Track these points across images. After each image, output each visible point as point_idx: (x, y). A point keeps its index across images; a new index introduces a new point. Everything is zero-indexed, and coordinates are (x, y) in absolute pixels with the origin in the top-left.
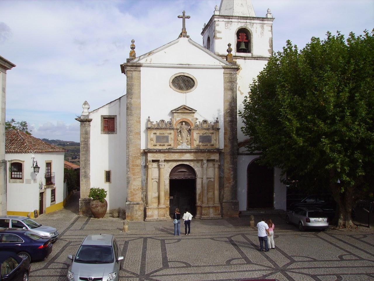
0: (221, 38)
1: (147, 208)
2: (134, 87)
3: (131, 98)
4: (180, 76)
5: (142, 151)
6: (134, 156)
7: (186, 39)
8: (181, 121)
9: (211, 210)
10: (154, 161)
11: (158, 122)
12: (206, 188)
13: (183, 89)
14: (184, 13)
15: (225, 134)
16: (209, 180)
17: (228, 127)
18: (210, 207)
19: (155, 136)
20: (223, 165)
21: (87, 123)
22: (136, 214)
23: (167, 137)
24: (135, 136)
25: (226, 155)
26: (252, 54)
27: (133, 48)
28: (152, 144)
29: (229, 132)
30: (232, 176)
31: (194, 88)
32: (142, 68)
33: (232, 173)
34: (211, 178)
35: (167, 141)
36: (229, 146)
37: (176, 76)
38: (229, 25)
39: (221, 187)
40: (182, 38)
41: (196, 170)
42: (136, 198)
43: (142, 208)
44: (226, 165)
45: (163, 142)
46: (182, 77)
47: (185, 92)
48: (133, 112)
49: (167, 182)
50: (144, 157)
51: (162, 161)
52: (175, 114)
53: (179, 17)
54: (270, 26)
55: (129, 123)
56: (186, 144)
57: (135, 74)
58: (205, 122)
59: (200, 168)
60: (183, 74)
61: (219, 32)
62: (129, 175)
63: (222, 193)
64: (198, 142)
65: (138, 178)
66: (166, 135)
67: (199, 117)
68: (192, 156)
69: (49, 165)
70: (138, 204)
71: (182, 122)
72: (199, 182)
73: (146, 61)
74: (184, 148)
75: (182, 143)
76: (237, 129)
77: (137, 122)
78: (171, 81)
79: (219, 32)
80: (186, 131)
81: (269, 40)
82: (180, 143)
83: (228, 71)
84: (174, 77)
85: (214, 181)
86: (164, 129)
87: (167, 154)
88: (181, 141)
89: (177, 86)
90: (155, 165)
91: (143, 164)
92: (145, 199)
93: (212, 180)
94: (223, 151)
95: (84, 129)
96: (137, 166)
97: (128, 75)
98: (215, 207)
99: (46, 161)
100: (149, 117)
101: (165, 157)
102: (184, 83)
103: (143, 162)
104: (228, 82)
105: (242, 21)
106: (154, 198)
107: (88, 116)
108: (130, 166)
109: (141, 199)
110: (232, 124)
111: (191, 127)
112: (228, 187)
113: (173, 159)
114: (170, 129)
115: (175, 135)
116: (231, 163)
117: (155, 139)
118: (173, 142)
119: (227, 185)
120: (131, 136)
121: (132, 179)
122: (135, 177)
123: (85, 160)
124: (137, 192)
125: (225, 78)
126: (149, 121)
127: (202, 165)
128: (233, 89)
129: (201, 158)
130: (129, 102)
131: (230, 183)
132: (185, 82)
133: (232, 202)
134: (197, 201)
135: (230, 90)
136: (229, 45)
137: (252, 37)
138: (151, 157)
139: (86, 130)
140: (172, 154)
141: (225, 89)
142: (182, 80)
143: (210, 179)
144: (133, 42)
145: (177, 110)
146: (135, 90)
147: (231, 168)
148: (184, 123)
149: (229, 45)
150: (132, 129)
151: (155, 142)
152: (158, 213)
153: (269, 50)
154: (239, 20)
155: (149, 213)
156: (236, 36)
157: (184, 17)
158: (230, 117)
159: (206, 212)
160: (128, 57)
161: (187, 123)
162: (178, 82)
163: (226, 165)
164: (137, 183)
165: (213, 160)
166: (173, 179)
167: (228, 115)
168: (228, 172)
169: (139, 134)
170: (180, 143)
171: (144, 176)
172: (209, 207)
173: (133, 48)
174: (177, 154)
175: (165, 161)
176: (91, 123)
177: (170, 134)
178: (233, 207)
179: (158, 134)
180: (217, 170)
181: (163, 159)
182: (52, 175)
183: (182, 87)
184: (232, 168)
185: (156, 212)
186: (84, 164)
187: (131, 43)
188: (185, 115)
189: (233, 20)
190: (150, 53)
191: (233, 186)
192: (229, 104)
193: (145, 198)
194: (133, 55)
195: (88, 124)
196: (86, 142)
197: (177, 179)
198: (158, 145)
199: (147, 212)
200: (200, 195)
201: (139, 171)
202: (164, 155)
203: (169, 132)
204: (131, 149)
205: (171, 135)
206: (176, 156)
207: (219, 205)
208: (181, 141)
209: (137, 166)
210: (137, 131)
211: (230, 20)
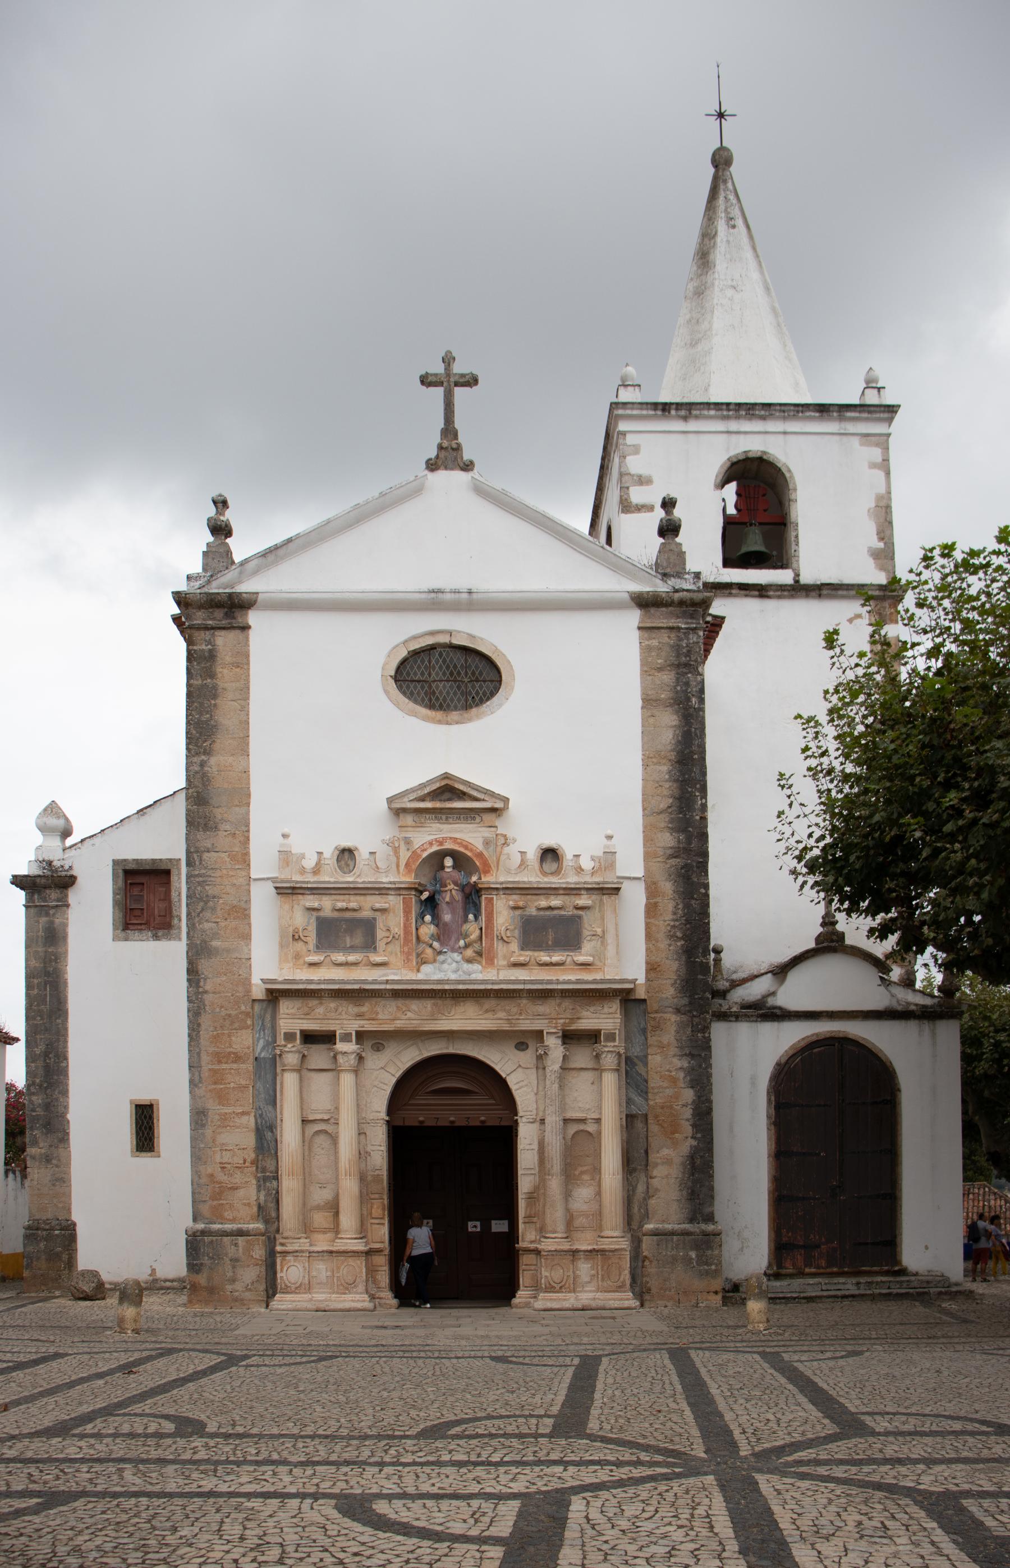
1: (279, 1248)
3: (208, 752)
4: (432, 648)
5: (258, 992)
6: (224, 1013)
7: (458, 476)
8: (435, 848)
9: (584, 1269)
10: (310, 1038)
12: (556, 1164)
13: (448, 706)
15: (651, 910)
16: (573, 1129)
17: (666, 880)
18: (577, 1251)
20: (644, 1059)
22: (233, 1280)
24: (223, 924)
25: (656, 1012)
28: (297, 956)
29: (669, 906)
30: (688, 1113)
31: (495, 699)
32: (253, 618)
33: (689, 1095)
35: (370, 944)
36: (672, 967)
39: (634, 1161)
40: (442, 476)
42: (231, 1206)
43: (259, 1252)
44: (658, 1058)
45: (353, 949)
46: (441, 655)
47: (455, 715)
48: (218, 813)
50: (268, 1017)
51: (347, 1037)
55: (197, 863)
57: (224, 640)
58: (550, 856)
59: (532, 1075)
63: (641, 1188)
64: (514, 946)
65: (243, 1113)
67: (525, 833)
68: (487, 1011)
70: (240, 1233)
71: (440, 856)
72: (526, 1136)
75: (440, 953)
76: (706, 886)
77: (233, 857)
82: (429, 951)
83: (661, 619)
84: (403, 653)
85: (599, 1133)
89: (418, 693)
90: (318, 1057)
91: (263, 1048)
92: (269, 1212)
93: (591, 1128)
94: (641, 994)
96: (238, 1058)
97: (195, 648)
98: (603, 1251)
101: (360, 1016)
102: (450, 677)
103: (261, 1043)
104: (660, 669)
106: (318, 1208)
109: (255, 1209)
110: (685, 866)
111: (480, 878)
112: (668, 1162)
113: (399, 1024)
116: (681, 1048)
117: (312, 938)
118: (396, 947)
120: (207, 926)
121: (217, 1117)
124: (238, 1178)
125: (646, 651)
127: (540, 1058)
128: (689, 699)
129: (537, 1025)
130: (197, 768)
131: (675, 1144)
132: (459, 673)
133: (685, 1233)
134: (521, 1226)
135: (671, 705)
141: (648, 702)
142: (441, 668)
143: (582, 1127)
146: (225, 714)
147: (681, 1075)
148: (448, 862)
150: (210, 890)
152: (329, 1273)
155: (290, 1272)
157: (449, 381)
158: (672, 830)
159: (557, 1274)
161: (461, 861)
162: (422, 674)
163: (655, 1060)
165: (593, 1037)
166: (407, 1124)
167: (663, 821)
168: (669, 1092)
169: (241, 912)
171: (270, 1108)
172: (574, 1253)
174: (415, 1005)
175: (361, 1036)
178: (693, 1254)
179: (327, 912)
181: (354, 1026)
183: (445, 700)
184: (689, 1071)
185: (322, 1269)
187: (211, 511)
188: (451, 820)
191: (692, 1157)
192: (670, 772)
193: (272, 1205)
199: (278, 1267)
200: (532, 1197)
201: (243, 1082)
202: (356, 1010)
206: (412, 1016)
207: (624, 1244)
209: (238, 1058)
210: (235, 903)
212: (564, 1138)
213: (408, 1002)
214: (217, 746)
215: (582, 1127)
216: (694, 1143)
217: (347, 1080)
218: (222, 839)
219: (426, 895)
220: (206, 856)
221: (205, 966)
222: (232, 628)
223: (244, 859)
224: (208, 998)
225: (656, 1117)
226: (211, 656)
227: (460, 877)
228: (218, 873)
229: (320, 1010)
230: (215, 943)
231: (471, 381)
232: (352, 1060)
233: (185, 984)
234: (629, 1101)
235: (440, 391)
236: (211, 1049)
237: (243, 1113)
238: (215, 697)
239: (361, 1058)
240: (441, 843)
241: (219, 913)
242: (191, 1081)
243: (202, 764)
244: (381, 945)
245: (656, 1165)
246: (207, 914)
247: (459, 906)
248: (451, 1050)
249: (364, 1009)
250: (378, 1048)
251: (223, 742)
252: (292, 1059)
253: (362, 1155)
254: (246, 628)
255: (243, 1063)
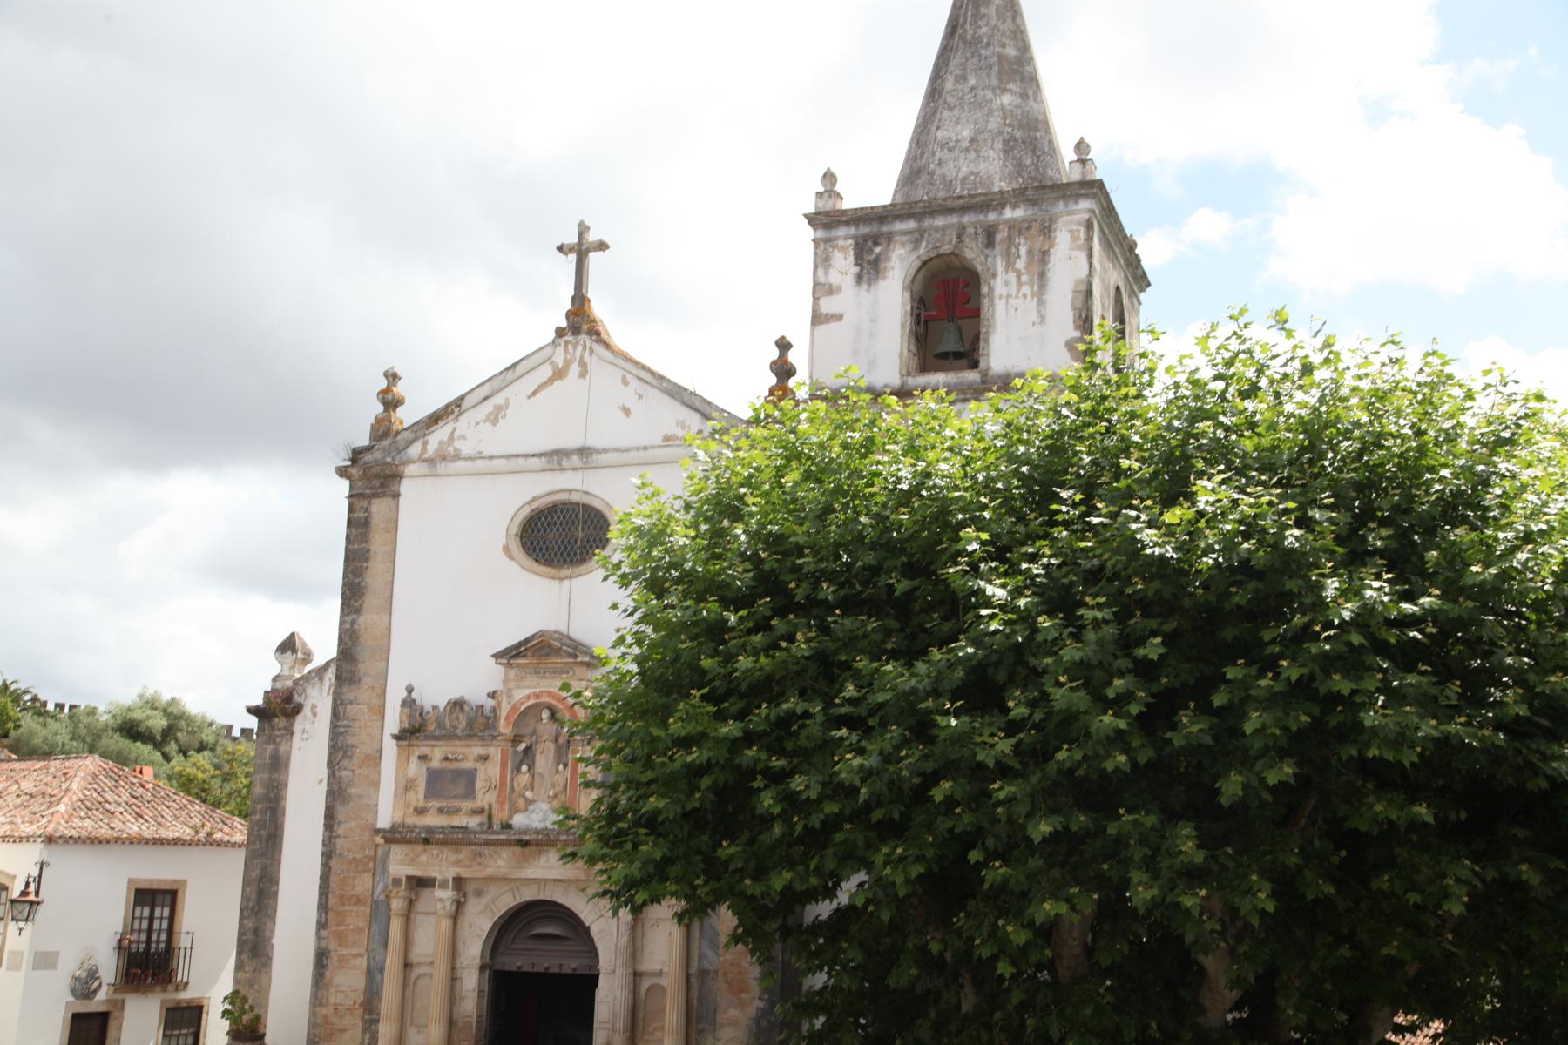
0: (839, 317)
2: (370, 564)
3: (358, 611)
8: (532, 702)
11: (442, 708)
14: (583, 230)
19: (424, 771)
21: (280, 722)
23: (470, 776)
26: (985, 374)
27: (390, 402)
28: (407, 805)
34: (660, 973)
35: (470, 793)
37: (535, 505)
38: (877, 250)
41: (594, 931)
47: (566, 572)
48: (361, 667)
49: (471, 981)
51: (444, 885)
52: (512, 673)
53: (560, 249)
54: (1078, 224)
56: (545, 806)
57: (379, 508)
60: (563, 497)
61: (831, 290)
62: (324, 943)
65: (359, 955)
66: (468, 765)
69: (156, 900)
71: (536, 708)
73: (424, 449)
74: (537, 824)
75: (531, 802)
77: (371, 709)
78: (515, 528)
79: (831, 290)
80: (551, 746)
81: (1070, 296)
84: (527, 511)
86: (460, 739)
87: (465, 852)
88: (529, 794)
93: (664, 982)
95: (270, 748)
96: (359, 901)
99: (130, 881)
100: (410, 690)
101: (458, 863)
105: (940, 221)
107: (288, 697)
108: (332, 901)
112: (735, 1023)
113: (489, 871)
114: (482, 739)
115: (503, 765)
119: (732, 1012)
120: (344, 773)
122: (345, 951)
123: (261, 878)
124: (347, 1021)
126: (408, 703)
131: (742, 1005)
136: (784, 345)
137: (985, 290)
138: (400, 864)
139: (277, 750)
140: (487, 850)
143: (656, 980)
144: (392, 377)
145: (518, 656)
146: (374, 577)
148: (545, 714)
149: (784, 345)
150: (350, 740)
151: (421, 796)
153: (1070, 345)
154: (927, 222)
156: (908, 295)
157: (581, 251)
160: (364, 441)
164: (349, 981)
169: (375, 759)
170: (521, 803)
171: (381, 950)
173: (390, 402)
175: (459, 882)
176: (300, 724)
177: (485, 758)
179: (436, 763)
180: (677, 932)
181: (451, 873)
182: (183, 941)
186: (254, 896)
189: (899, 226)
190: (435, 419)
191: (757, 1020)
194: (382, 430)
195: (285, 729)
196: (268, 800)
197: (526, 969)
198: (434, 810)
201: (361, 924)
203: (479, 750)
204: (340, 830)
205: (489, 766)
208: (529, 794)
209: (359, 901)
211: (885, 229)
212: (635, 991)
213: (498, 849)
214: (365, 606)
215: (656, 980)
216: (761, 1005)
217: (446, 924)
218: (363, 693)
219: (523, 746)
220: (349, 707)
221: (341, 811)
222: (384, 495)
223: (380, 711)
224: (339, 842)
225: (725, 974)
226: (366, 523)
227: (553, 727)
228: (357, 724)
229: (424, 858)
230: (352, 791)
231: (602, 246)
232: (450, 907)
233: (322, 828)
234: (701, 956)
235: (573, 257)
236: (338, 892)
237: (359, 955)
238: (367, 560)
239: (459, 905)
240: (537, 696)
241: (355, 761)
242: (318, 922)
243: (353, 623)
244: (479, 793)
245: (723, 1026)
246: (346, 762)
247: (552, 755)
248: (541, 897)
249: (461, 856)
250: (479, 893)
251: (371, 601)
252: (397, 905)
253: (453, 997)
254: (396, 496)
255: (364, 904)
